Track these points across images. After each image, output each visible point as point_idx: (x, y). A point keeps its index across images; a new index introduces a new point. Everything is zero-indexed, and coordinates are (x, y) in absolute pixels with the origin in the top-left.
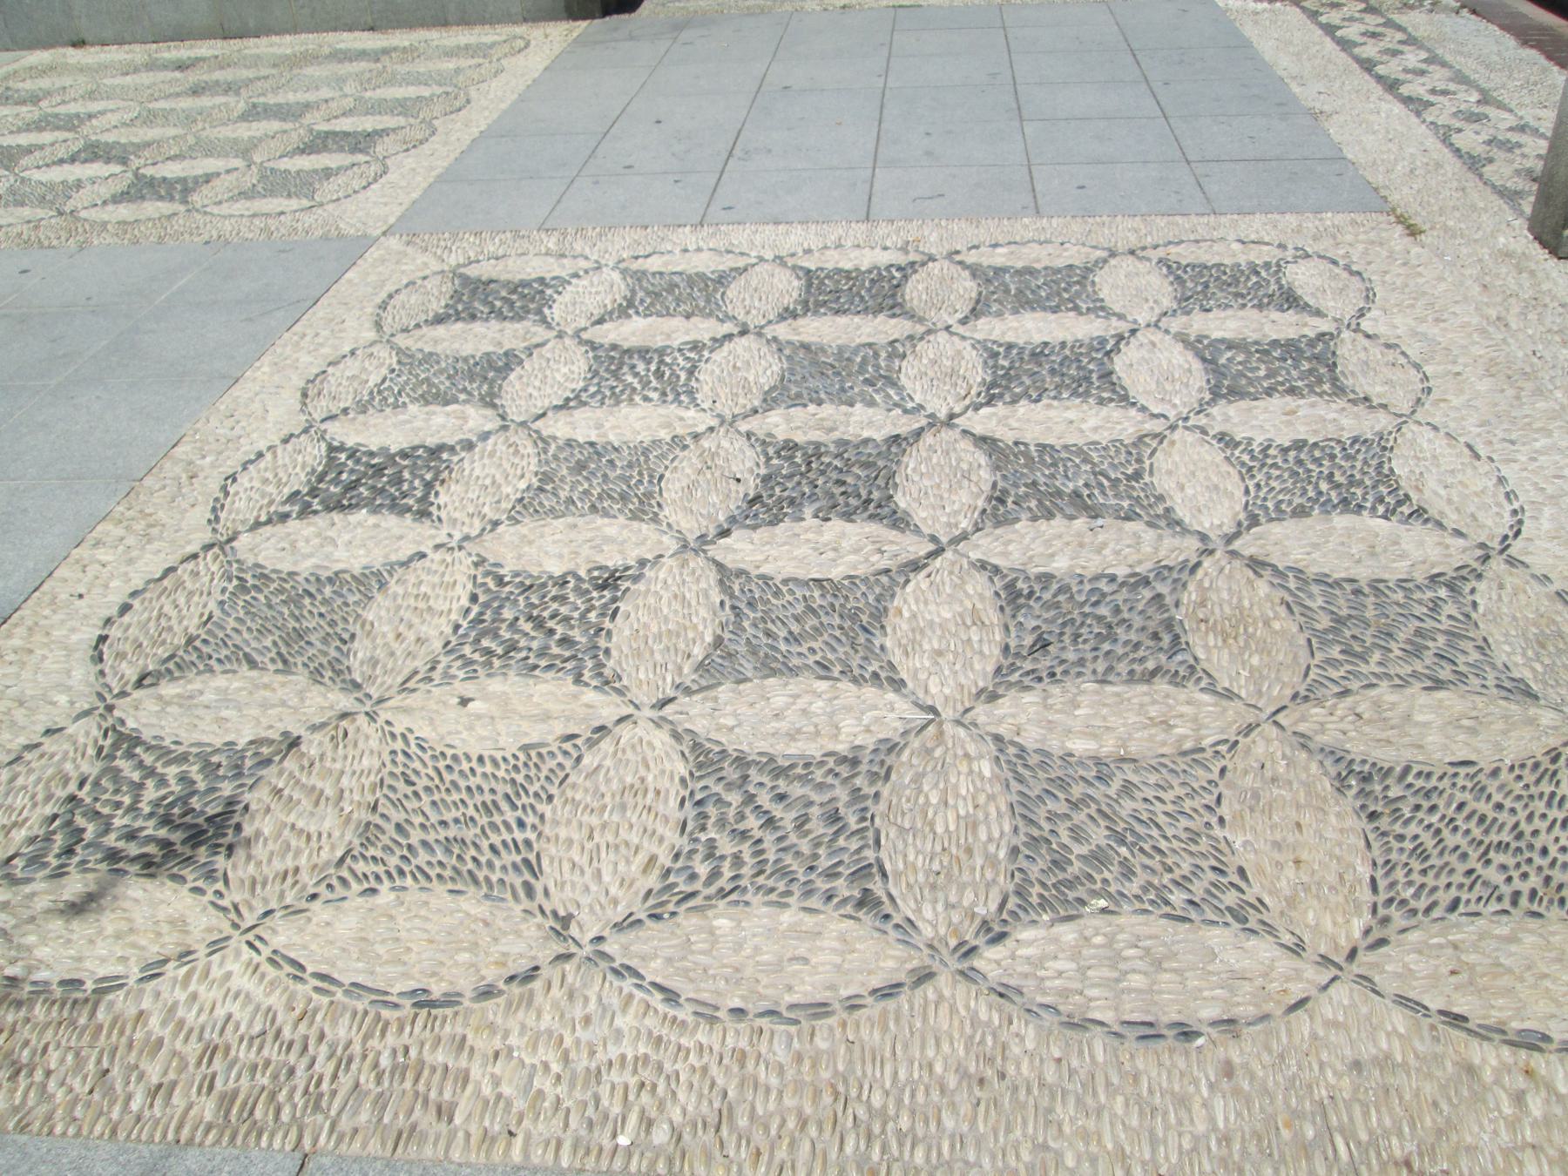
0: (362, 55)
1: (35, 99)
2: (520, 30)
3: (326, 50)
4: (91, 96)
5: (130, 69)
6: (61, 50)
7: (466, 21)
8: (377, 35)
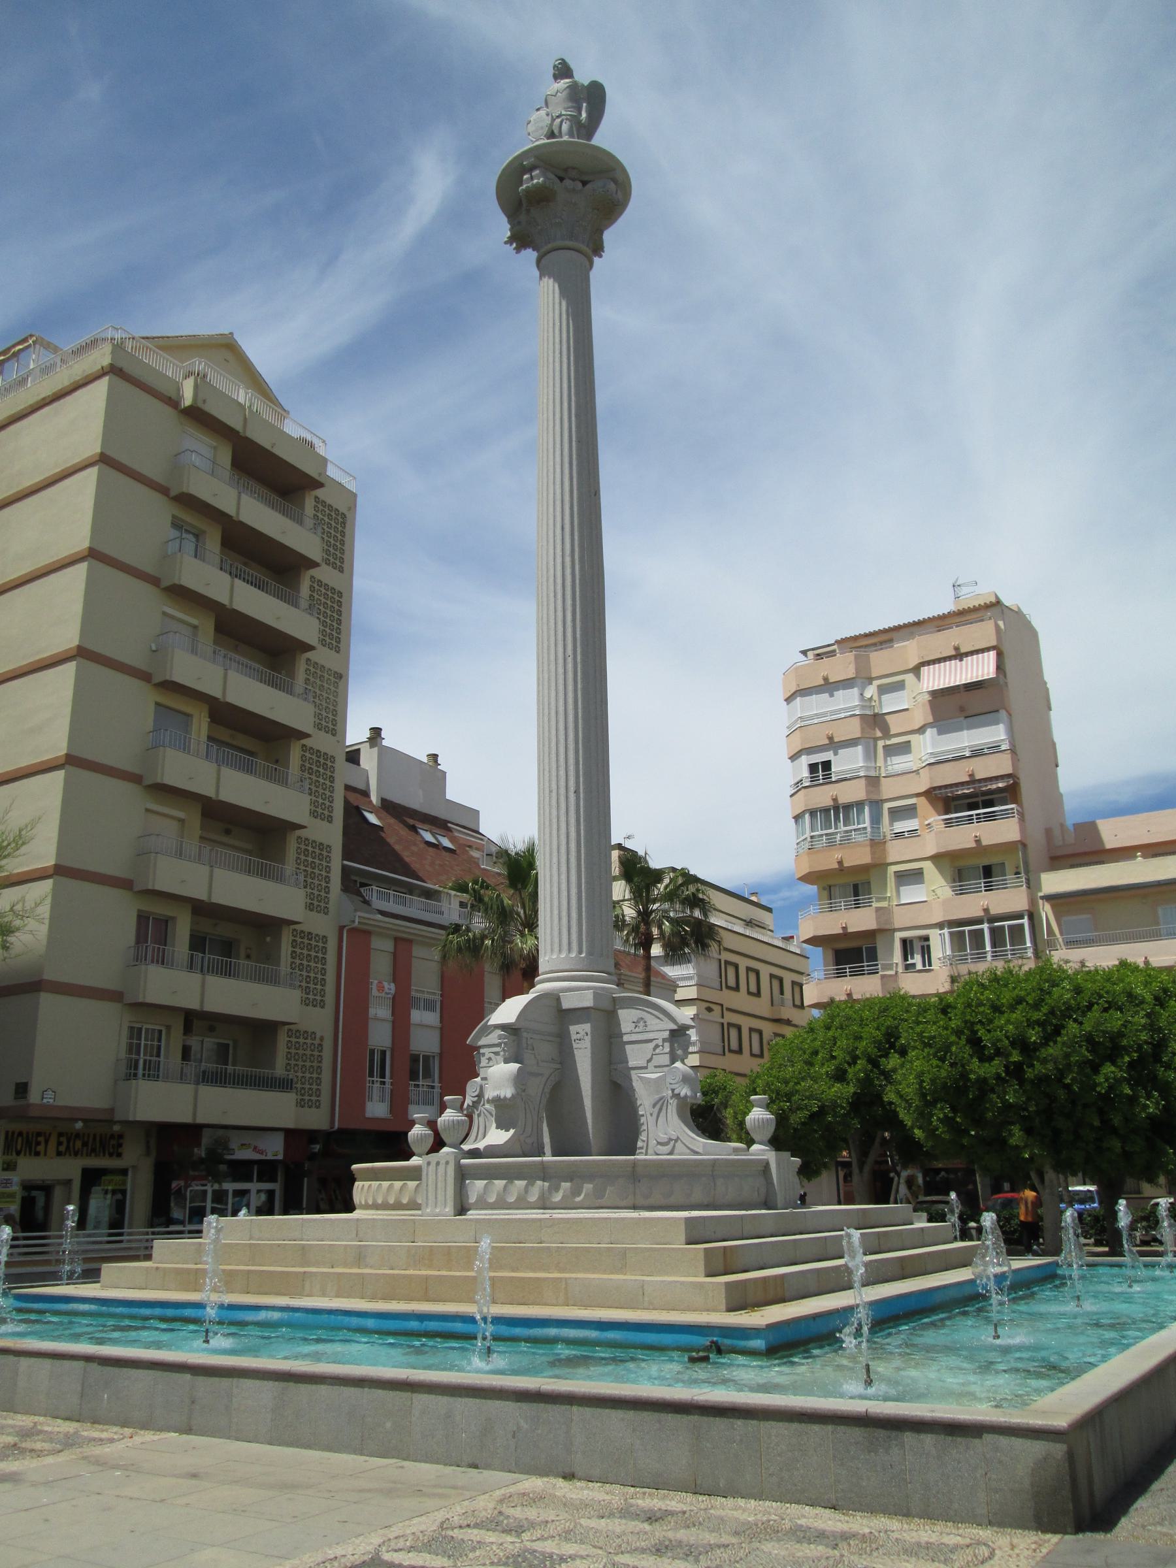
0: (821, 1536)
1: (518, 1529)
2: (984, 1533)
3: (787, 1525)
4: (567, 1535)
5: (605, 1513)
6: (553, 1480)
7: (928, 1514)
8: (838, 1515)
